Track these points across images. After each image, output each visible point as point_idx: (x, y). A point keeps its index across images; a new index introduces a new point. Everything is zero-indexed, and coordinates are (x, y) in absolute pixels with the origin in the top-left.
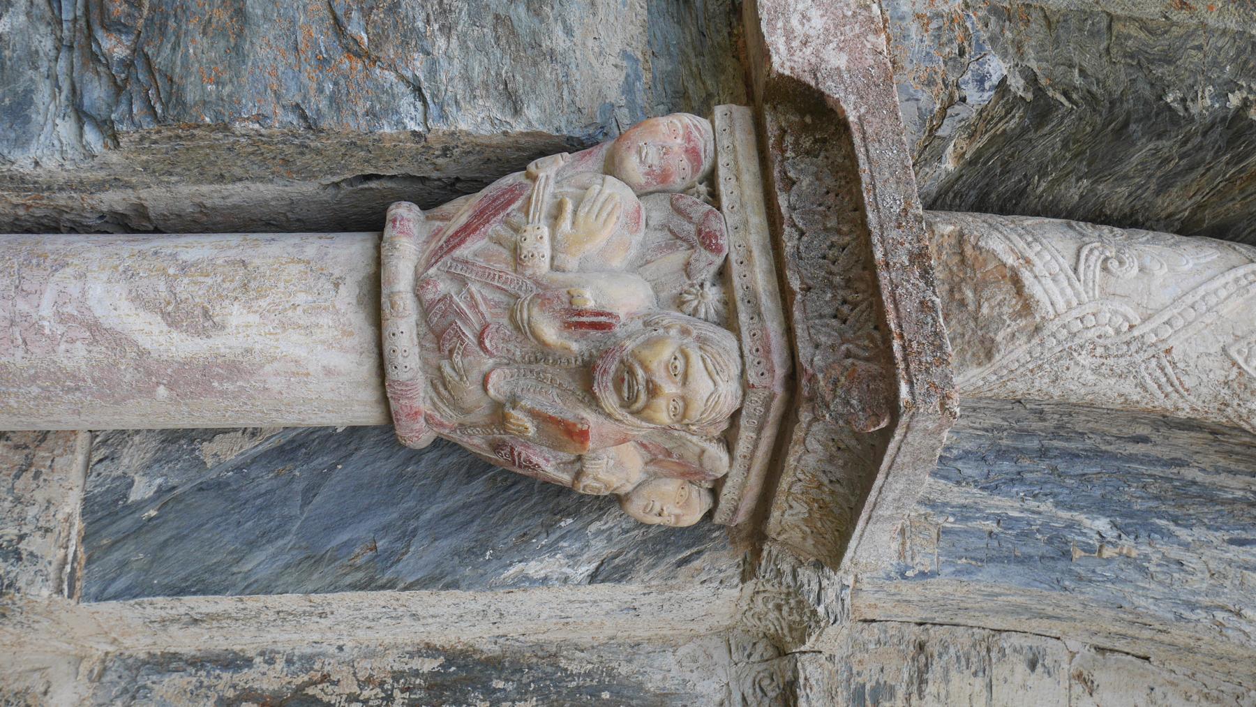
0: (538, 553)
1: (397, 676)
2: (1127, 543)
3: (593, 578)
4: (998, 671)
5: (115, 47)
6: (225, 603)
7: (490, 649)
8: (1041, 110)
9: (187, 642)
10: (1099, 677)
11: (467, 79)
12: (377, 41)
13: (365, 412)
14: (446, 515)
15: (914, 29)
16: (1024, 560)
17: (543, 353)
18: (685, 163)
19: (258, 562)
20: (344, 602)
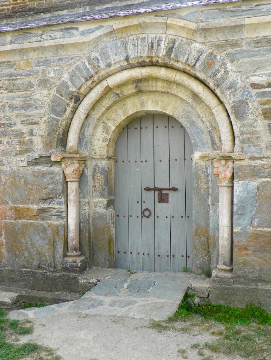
2: (86, 138)
5: (58, 196)
6: (89, 190)
8: (61, 145)
10: (94, 138)
12: (57, 182)
13: (78, 182)
16: (87, 144)
17: (75, 173)
19: (86, 189)
20: (89, 184)
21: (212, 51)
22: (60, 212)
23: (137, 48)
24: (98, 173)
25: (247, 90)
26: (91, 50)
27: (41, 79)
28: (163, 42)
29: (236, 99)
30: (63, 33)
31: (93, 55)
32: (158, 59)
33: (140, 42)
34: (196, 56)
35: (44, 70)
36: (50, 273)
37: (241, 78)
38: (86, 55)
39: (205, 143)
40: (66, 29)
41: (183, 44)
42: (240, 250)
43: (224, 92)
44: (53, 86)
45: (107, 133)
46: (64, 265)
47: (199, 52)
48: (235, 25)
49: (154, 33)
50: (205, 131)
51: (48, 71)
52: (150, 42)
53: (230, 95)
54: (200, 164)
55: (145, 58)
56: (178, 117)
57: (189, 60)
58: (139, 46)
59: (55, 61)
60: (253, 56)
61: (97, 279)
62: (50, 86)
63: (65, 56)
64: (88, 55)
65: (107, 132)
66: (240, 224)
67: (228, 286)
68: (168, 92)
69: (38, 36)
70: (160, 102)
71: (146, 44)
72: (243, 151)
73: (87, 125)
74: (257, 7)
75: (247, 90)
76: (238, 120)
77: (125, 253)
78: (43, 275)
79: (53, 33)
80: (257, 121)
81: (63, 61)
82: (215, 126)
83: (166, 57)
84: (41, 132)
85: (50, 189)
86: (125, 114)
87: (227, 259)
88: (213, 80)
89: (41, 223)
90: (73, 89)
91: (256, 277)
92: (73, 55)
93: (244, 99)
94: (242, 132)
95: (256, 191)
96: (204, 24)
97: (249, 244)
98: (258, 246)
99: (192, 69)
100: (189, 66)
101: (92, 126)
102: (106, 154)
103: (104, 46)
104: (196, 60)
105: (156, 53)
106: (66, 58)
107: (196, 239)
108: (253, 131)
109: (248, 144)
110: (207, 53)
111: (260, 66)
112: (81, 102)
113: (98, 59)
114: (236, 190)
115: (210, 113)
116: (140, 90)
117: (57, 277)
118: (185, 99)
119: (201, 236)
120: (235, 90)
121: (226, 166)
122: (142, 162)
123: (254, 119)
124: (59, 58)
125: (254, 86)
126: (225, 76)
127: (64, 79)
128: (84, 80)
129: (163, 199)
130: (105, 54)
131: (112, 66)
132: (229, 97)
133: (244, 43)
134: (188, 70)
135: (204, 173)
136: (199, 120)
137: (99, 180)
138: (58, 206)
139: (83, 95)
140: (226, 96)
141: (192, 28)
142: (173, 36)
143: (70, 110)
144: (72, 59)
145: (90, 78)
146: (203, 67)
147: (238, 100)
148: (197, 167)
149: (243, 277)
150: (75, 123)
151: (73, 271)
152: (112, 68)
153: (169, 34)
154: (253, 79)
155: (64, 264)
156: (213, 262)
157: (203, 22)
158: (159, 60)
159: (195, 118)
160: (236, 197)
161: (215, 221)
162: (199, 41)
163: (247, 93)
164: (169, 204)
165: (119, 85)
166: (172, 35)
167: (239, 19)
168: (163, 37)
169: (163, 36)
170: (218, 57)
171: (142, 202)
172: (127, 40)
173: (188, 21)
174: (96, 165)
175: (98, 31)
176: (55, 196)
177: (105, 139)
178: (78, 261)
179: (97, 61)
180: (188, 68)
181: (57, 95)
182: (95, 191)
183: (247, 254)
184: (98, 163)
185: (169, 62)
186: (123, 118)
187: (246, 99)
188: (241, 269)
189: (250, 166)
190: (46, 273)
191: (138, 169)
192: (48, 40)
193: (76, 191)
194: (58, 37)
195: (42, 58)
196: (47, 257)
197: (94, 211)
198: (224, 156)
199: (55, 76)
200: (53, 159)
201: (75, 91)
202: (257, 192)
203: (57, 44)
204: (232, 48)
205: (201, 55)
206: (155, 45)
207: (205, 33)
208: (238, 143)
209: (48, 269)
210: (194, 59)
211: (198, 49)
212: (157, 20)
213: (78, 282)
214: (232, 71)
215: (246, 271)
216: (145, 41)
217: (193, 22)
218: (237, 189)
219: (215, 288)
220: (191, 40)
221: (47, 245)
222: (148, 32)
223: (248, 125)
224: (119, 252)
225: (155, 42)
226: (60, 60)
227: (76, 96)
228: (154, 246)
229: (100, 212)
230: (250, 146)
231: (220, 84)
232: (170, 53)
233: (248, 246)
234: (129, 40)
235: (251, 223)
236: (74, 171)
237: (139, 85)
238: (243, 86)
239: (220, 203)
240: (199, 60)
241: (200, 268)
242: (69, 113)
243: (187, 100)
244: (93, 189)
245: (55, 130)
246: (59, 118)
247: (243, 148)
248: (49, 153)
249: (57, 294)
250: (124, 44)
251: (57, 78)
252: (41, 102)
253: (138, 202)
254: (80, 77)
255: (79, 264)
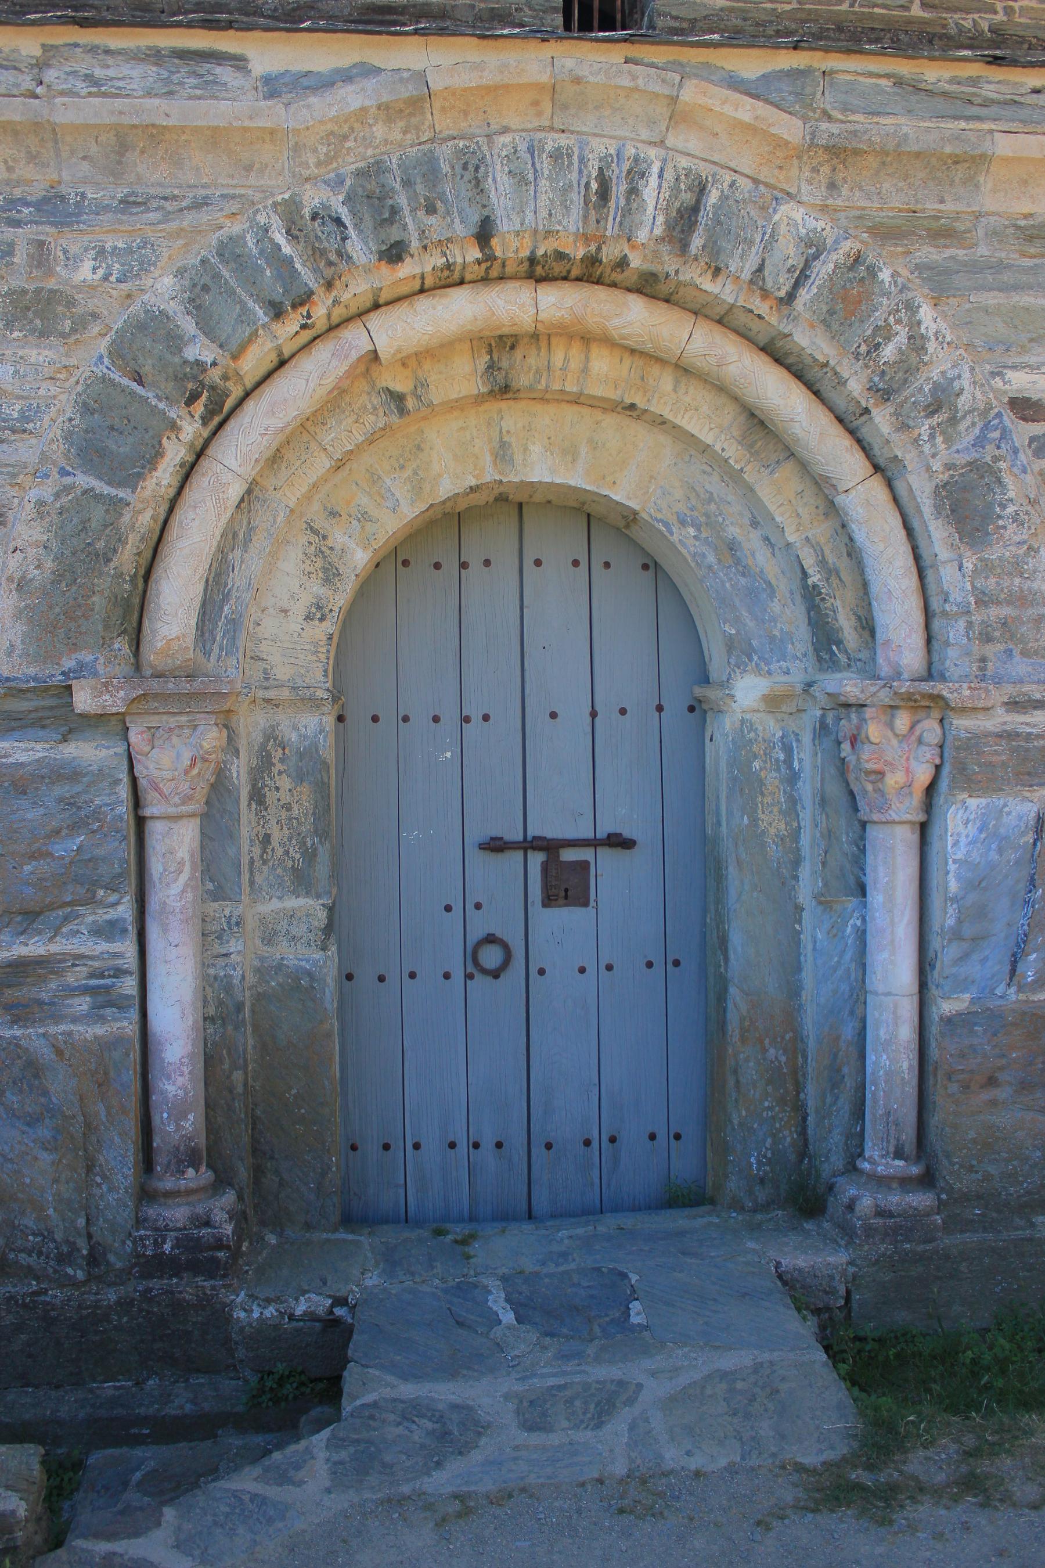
0: (231, 774)
1: (257, 814)
2: (232, 602)
3: (238, 758)
4: (260, 636)
7: (249, 788)
9: (247, 876)
10: (263, 605)
11: (110, 795)
14: (218, 800)
15: (108, 669)
16: (235, 631)
17: (199, 773)
18: (145, 736)
21: (858, 246)
22: (110, 976)
23: (532, 193)
24: (280, 773)
25: (996, 421)
26: (306, 173)
27: (24, 292)
28: (653, 181)
29: (956, 455)
30: (165, 74)
31: (313, 198)
32: (627, 251)
33: (545, 165)
34: (796, 261)
35: (41, 244)
36: (68, 1291)
37: (972, 369)
38: (273, 195)
39: (781, 640)
40: (183, 55)
41: (737, 201)
42: (968, 1087)
43: (911, 423)
44: (96, 329)
45: (327, 581)
46: (144, 1246)
47: (808, 245)
48: (958, 151)
49: (611, 137)
50: (782, 587)
51: (65, 252)
52: (594, 173)
53: (932, 437)
54: (760, 728)
55: (571, 239)
56: (661, 521)
57: (766, 273)
58: (544, 183)
59: (107, 208)
60: (1016, 288)
61: (329, 1296)
62: (73, 331)
63: (160, 185)
64: (286, 196)
65: (330, 575)
66: (966, 979)
67: (925, 1242)
68: (632, 407)
69: (15, 68)
70: (584, 450)
71: (574, 176)
72: (984, 675)
73: (241, 536)
74: (1035, 96)
75: (996, 421)
76: (967, 543)
77: (386, 1147)
78: (25, 1306)
79: (108, 67)
80: (1037, 551)
81: (148, 210)
82: (838, 564)
83: (664, 248)
84: (14, 562)
85: (62, 858)
86: (417, 490)
87: (908, 1135)
88: (867, 366)
89: (15, 1038)
90: (202, 351)
91: (1028, 1193)
92: (204, 186)
93: (988, 459)
94: (980, 596)
95: (1031, 841)
96: (835, 129)
97: (1004, 1061)
98: (1040, 1066)
99: (779, 310)
100: (765, 294)
101: (259, 541)
102: (322, 679)
103: (371, 161)
104: (796, 275)
105: (621, 224)
106: (165, 199)
107: (747, 1060)
108: (1022, 591)
109: (1000, 647)
110: (841, 252)
111: (1042, 331)
112: (221, 425)
113: (338, 221)
114: (955, 837)
115: (817, 507)
116: (506, 387)
117: (110, 1307)
118: (709, 441)
119: (767, 1041)
120: (953, 421)
121: (913, 738)
122: (467, 720)
123: (1025, 542)
124: (126, 196)
125: (1024, 410)
126: (914, 359)
127: (153, 300)
128: (265, 314)
129: (566, 890)
130: (377, 202)
131: (408, 260)
132: (928, 445)
133: (981, 232)
134: (760, 317)
135: (778, 770)
136: (755, 536)
137: (288, 808)
138: (103, 946)
139: (244, 385)
140: (916, 440)
141: (790, 139)
142: (697, 161)
143: (181, 455)
144: (201, 204)
145: (294, 307)
146: (825, 308)
147: (964, 462)
148: (751, 740)
149: (979, 1197)
150: (197, 522)
151: (195, 1267)
152: (407, 269)
153: (681, 153)
154: (1020, 382)
155: (142, 1238)
156: (830, 1150)
157: (830, 118)
158: (631, 256)
159: (738, 531)
160: (958, 869)
161: (839, 973)
162: (805, 199)
163: (996, 434)
164: (591, 910)
165: (408, 357)
166: (689, 155)
167: (970, 130)
168: (653, 157)
169: (652, 153)
170: (885, 275)
171: (470, 906)
172: (485, 148)
173: (771, 103)
174: (271, 735)
175: (350, 88)
176: (89, 895)
177: (319, 607)
178: (219, 1216)
179: (331, 227)
180: (762, 307)
181: (116, 376)
182: (265, 862)
183: (993, 1103)
184: (278, 724)
185: (677, 272)
186: (410, 511)
187: (996, 459)
188: (973, 1166)
189: (1009, 736)
190: (45, 1292)
191: (448, 755)
192: (77, 95)
193: (194, 869)
194: (135, 87)
195: (29, 182)
196: (51, 1212)
197: (262, 959)
198: (913, 694)
199: (106, 278)
200: (84, 700)
201: (214, 364)
202: (1035, 844)
203: (126, 120)
204: (936, 247)
205: (816, 257)
206: (619, 190)
207: (834, 170)
208: (965, 641)
209: (56, 1271)
210: (789, 271)
211: (804, 231)
212: (634, 78)
213: (228, 1319)
214: (937, 339)
215: (993, 1172)
216: (571, 164)
217: (790, 113)
218: (959, 834)
219: (877, 1261)
220: (775, 188)
221: (46, 1149)
222: (585, 129)
223: (1002, 567)
224: (354, 1148)
225: (617, 173)
226: (135, 203)
227: (213, 388)
228: (525, 1105)
229: (291, 960)
230: (1009, 653)
231: (895, 386)
232: (683, 231)
233: (1001, 1069)
234: (495, 152)
235: (1013, 972)
236: (192, 766)
237: (505, 364)
238: (982, 406)
239: (876, 898)
240: (807, 277)
241: (762, 1181)
242: (171, 470)
243: (718, 448)
244: (257, 851)
245: (97, 555)
246: (121, 495)
247: (983, 660)
248: (63, 673)
249: (111, 1392)
250: (471, 168)
251: (114, 293)
252: (17, 407)
253: (448, 908)
254: (245, 297)
255: (228, 1229)
